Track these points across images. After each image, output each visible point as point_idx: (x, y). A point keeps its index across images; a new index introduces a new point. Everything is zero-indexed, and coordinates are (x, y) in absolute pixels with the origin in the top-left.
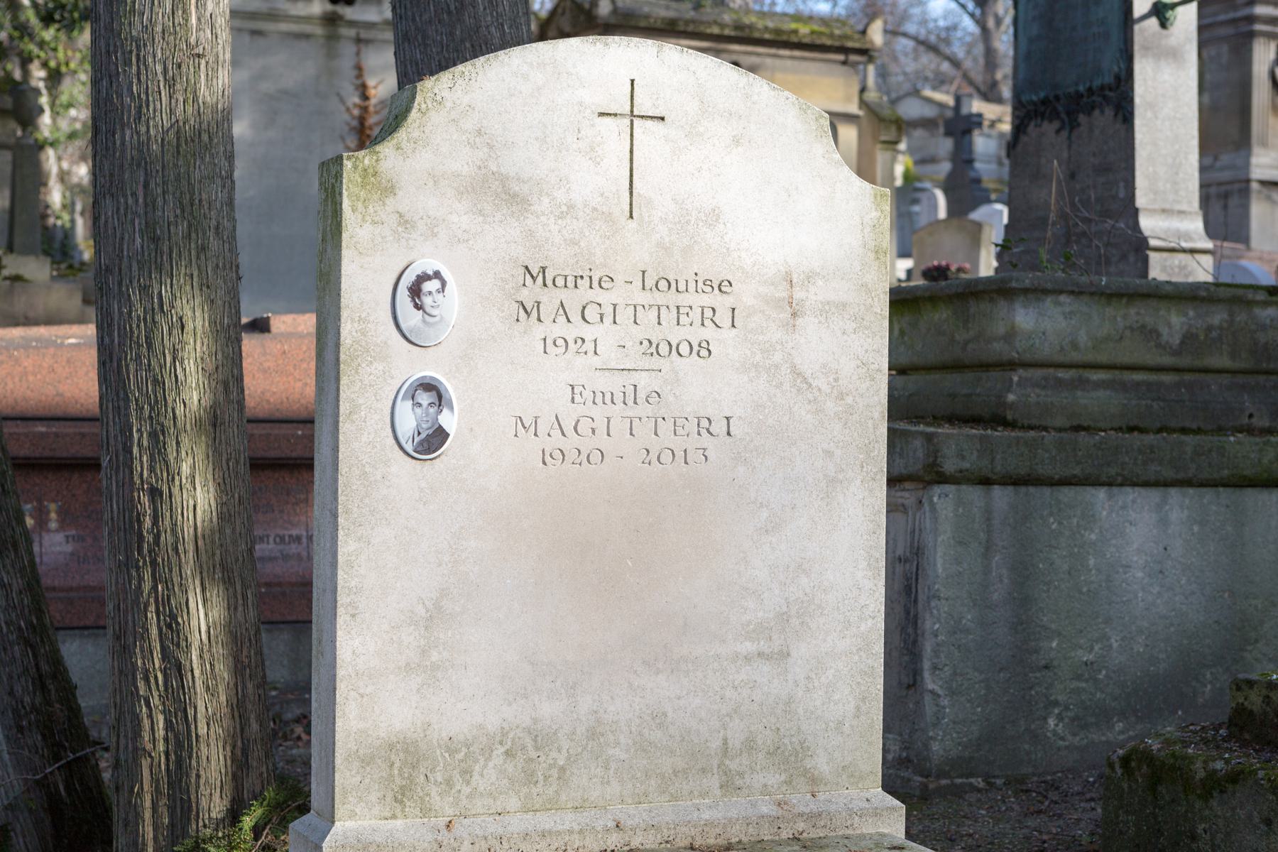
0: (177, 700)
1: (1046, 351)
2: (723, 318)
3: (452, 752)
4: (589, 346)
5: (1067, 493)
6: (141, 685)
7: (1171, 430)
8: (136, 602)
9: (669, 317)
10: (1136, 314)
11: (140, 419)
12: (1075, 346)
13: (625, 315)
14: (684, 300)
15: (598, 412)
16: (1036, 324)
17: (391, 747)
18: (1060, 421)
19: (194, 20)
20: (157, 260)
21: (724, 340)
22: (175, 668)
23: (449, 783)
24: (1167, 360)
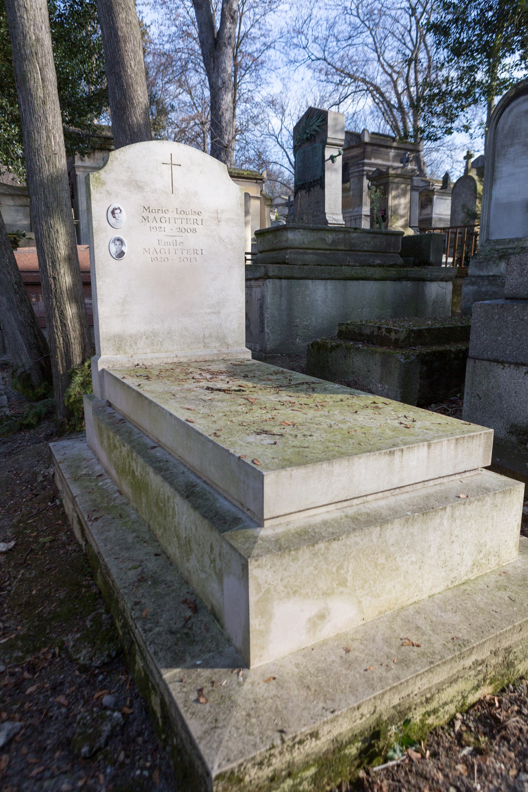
0: (65, 333)
1: (296, 244)
2: (199, 222)
3: (131, 337)
4: (163, 229)
5: (301, 281)
6: (55, 329)
7: (328, 265)
8: (52, 308)
9: (184, 222)
10: (320, 235)
11: (48, 258)
12: (304, 243)
13: (172, 221)
14: (189, 217)
15: (166, 247)
16: (294, 237)
17: (115, 336)
18: (300, 263)
19: (53, 143)
20: (49, 213)
21: (200, 228)
22: (64, 325)
23: (131, 345)
24: (328, 247)
